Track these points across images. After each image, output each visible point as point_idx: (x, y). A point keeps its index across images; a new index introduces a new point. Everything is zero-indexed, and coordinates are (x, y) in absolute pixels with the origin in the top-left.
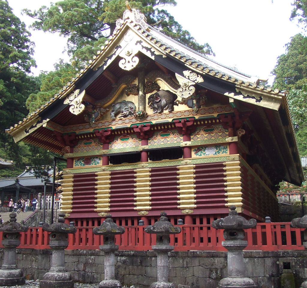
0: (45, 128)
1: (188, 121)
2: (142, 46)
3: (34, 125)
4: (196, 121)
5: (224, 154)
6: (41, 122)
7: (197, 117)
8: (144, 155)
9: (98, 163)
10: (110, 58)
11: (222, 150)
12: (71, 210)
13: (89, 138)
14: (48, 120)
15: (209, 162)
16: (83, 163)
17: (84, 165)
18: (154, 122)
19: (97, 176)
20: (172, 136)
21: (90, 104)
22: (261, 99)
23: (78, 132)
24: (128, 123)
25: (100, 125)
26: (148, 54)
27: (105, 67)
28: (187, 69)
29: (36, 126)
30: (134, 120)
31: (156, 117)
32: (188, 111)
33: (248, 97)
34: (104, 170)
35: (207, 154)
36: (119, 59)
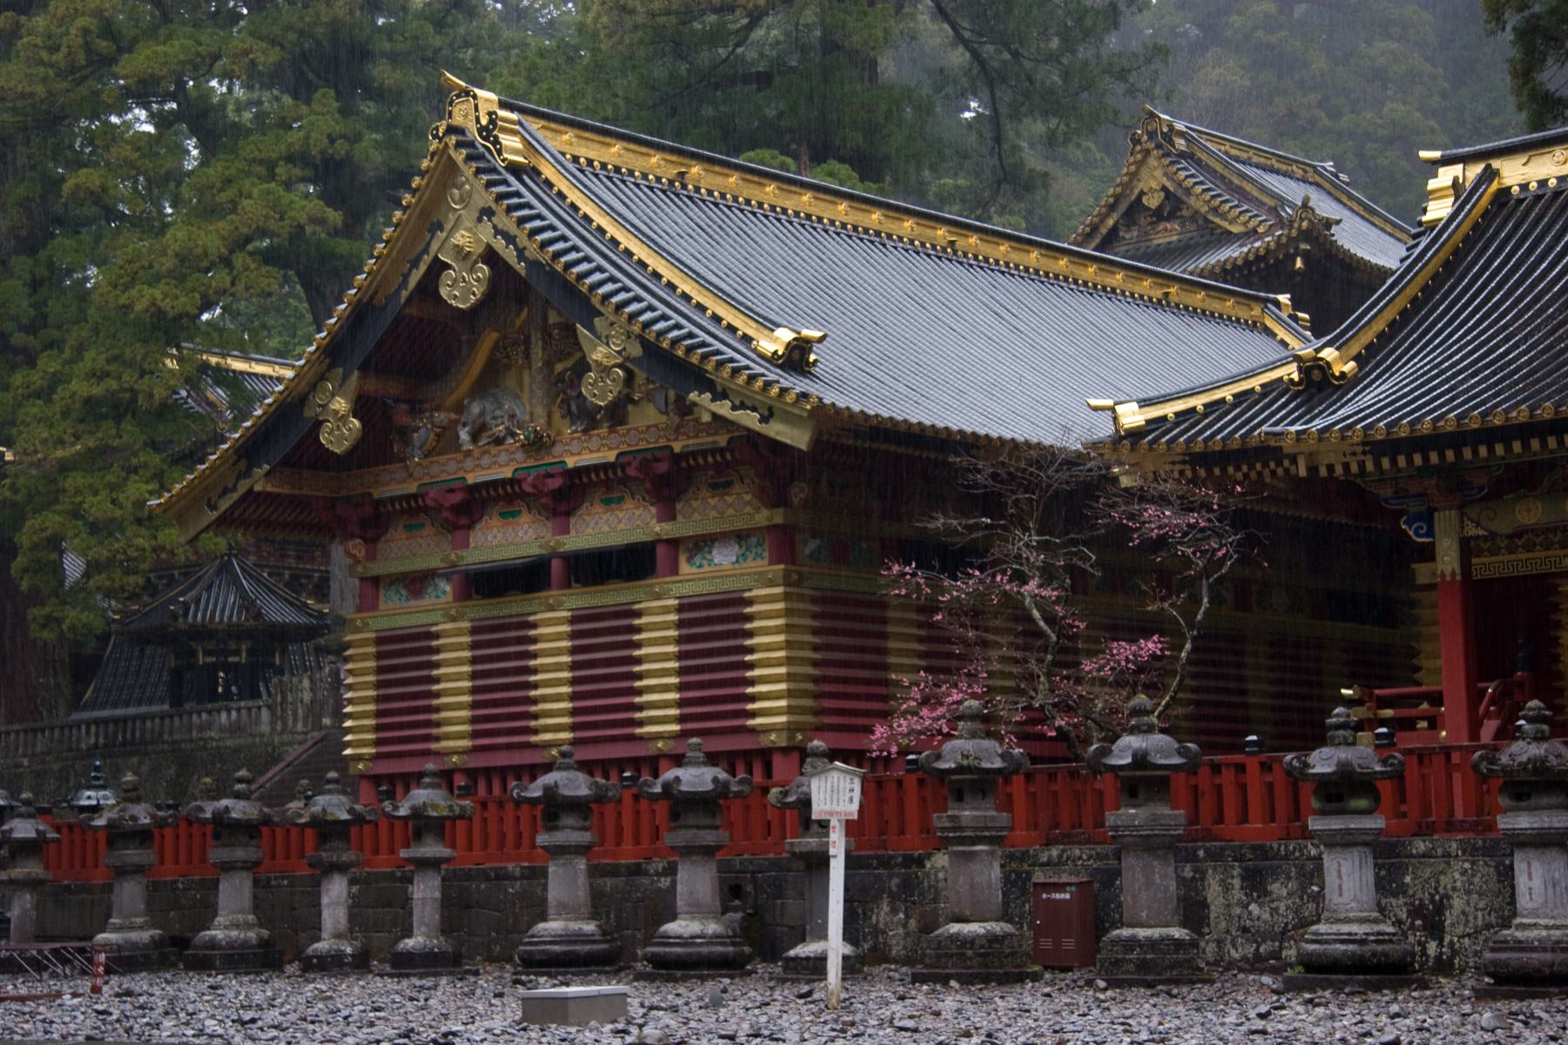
0: (259, 494)
1: (656, 460)
2: (495, 227)
3: (230, 486)
4: (677, 458)
5: (759, 562)
6: (247, 474)
7: (677, 447)
8: (556, 565)
9: (444, 593)
10: (415, 263)
11: (754, 550)
12: (372, 750)
13: (414, 509)
14: (267, 467)
15: (712, 589)
16: (404, 592)
17: (407, 599)
18: (571, 462)
19: (437, 636)
20: (629, 504)
21: (397, 400)
22: (771, 414)
23: (377, 493)
24: (501, 467)
25: (435, 469)
26: (510, 255)
27: (405, 294)
28: (600, 314)
29: (234, 489)
30: (520, 456)
31: (575, 447)
32: (655, 426)
33: (743, 406)
34: (454, 619)
35: (716, 561)
36: (438, 267)
